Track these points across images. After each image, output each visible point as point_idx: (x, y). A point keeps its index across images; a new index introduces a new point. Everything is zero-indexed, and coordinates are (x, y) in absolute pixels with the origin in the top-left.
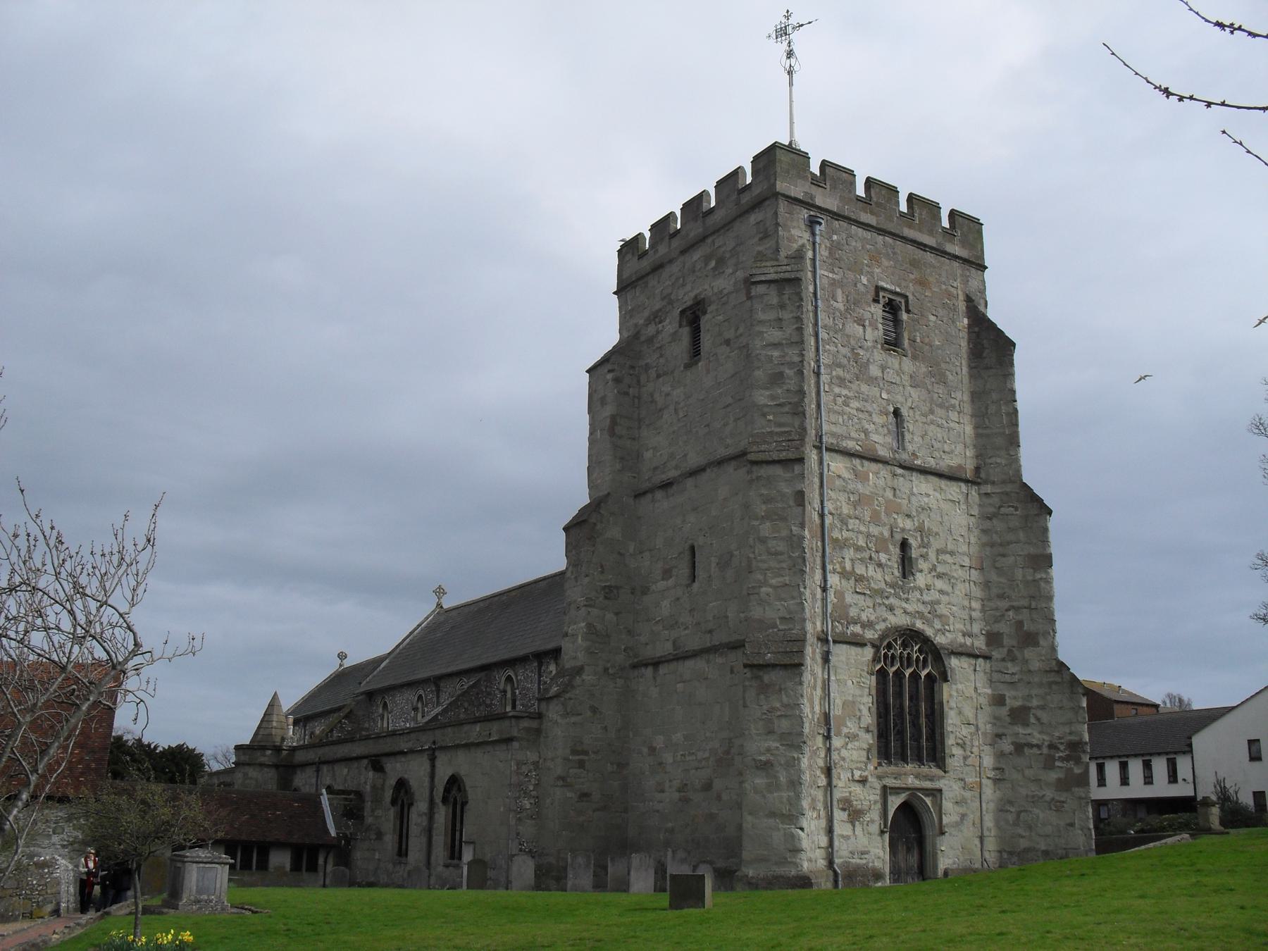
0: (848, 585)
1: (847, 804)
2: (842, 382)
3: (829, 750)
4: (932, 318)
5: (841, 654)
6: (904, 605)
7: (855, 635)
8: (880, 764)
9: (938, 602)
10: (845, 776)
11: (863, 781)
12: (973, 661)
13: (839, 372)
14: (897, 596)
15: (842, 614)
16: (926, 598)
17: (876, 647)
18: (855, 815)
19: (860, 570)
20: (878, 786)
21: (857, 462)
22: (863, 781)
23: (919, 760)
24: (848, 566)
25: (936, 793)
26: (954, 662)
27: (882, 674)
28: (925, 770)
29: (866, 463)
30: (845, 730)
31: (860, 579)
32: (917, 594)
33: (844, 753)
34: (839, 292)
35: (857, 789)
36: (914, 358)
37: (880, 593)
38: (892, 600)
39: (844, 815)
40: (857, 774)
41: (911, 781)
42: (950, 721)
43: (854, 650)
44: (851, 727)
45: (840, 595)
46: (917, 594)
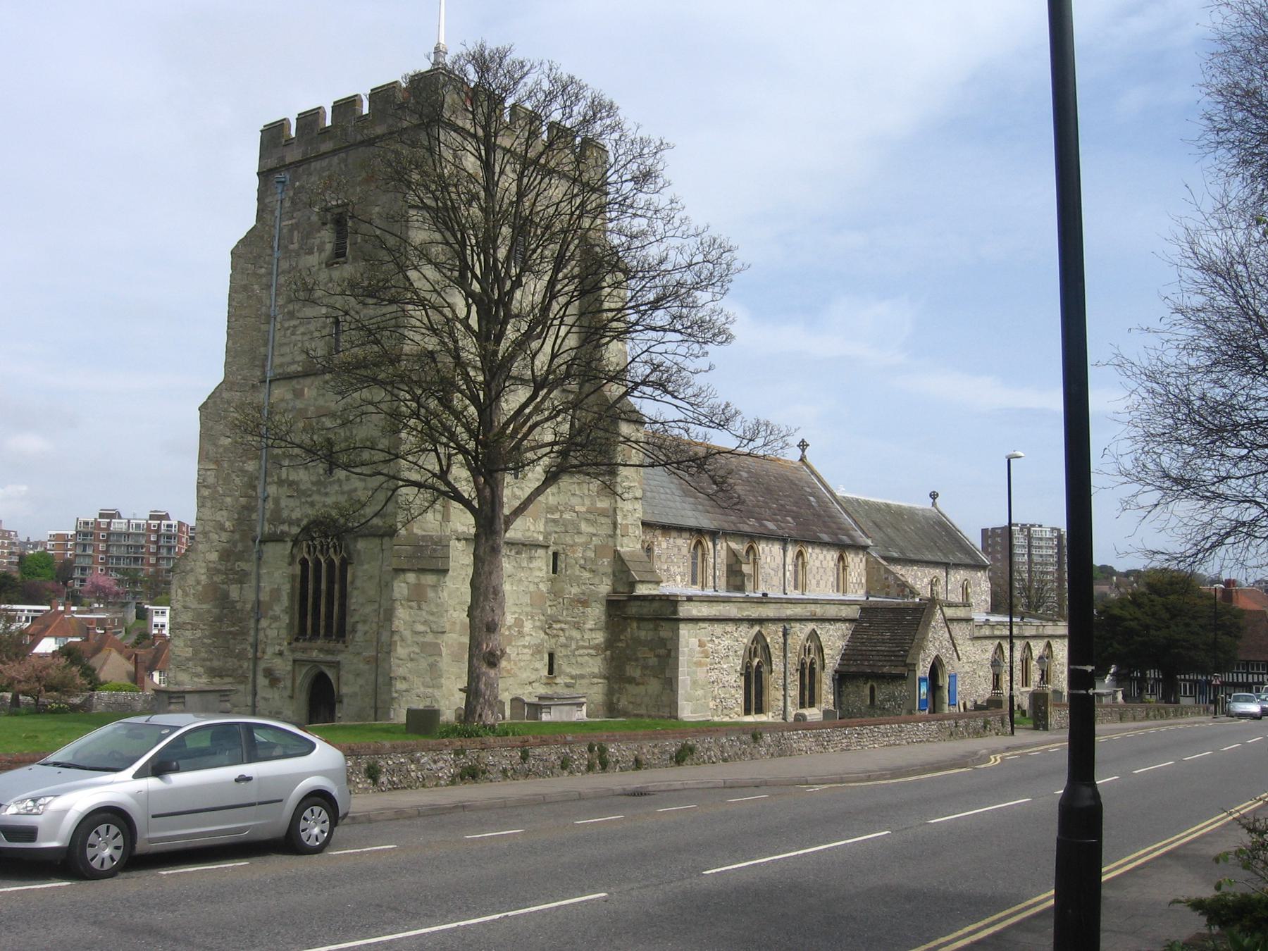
0: (285, 491)
1: (269, 673)
2: (291, 315)
3: (257, 630)
4: (377, 209)
5: (271, 550)
6: (323, 499)
7: (282, 532)
8: (297, 640)
9: (355, 490)
10: (270, 650)
11: (281, 654)
12: (377, 541)
13: (291, 307)
14: (319, 492)
15: (276, 518)
16: (346, 488)
17: (296, 542)
18: (274, 681)
19: (293, 476)
20: (291, 658)
21: (294, 382)
22: (281, 654)
23: (328, 634)
24: (284, 476)
25: (336, 665)
26: (361, 545)
27: (304, 563)
28: (332, 645)
29: (301, 380)
30: (271, 613)
31: (291, 484)
32: (336, 487)
33: (269, 632)
34: (296, 233)
35: (278, 662)
36: (355, 259)
37: (304, 493)
38: (316, 498)
39: (266, 682)
40: (277, 648)
41: (315, 654)
42: (354, 600)
43: (280, 546)
44: (277, 610)
45: (277, 501)
46: (336, 487)
